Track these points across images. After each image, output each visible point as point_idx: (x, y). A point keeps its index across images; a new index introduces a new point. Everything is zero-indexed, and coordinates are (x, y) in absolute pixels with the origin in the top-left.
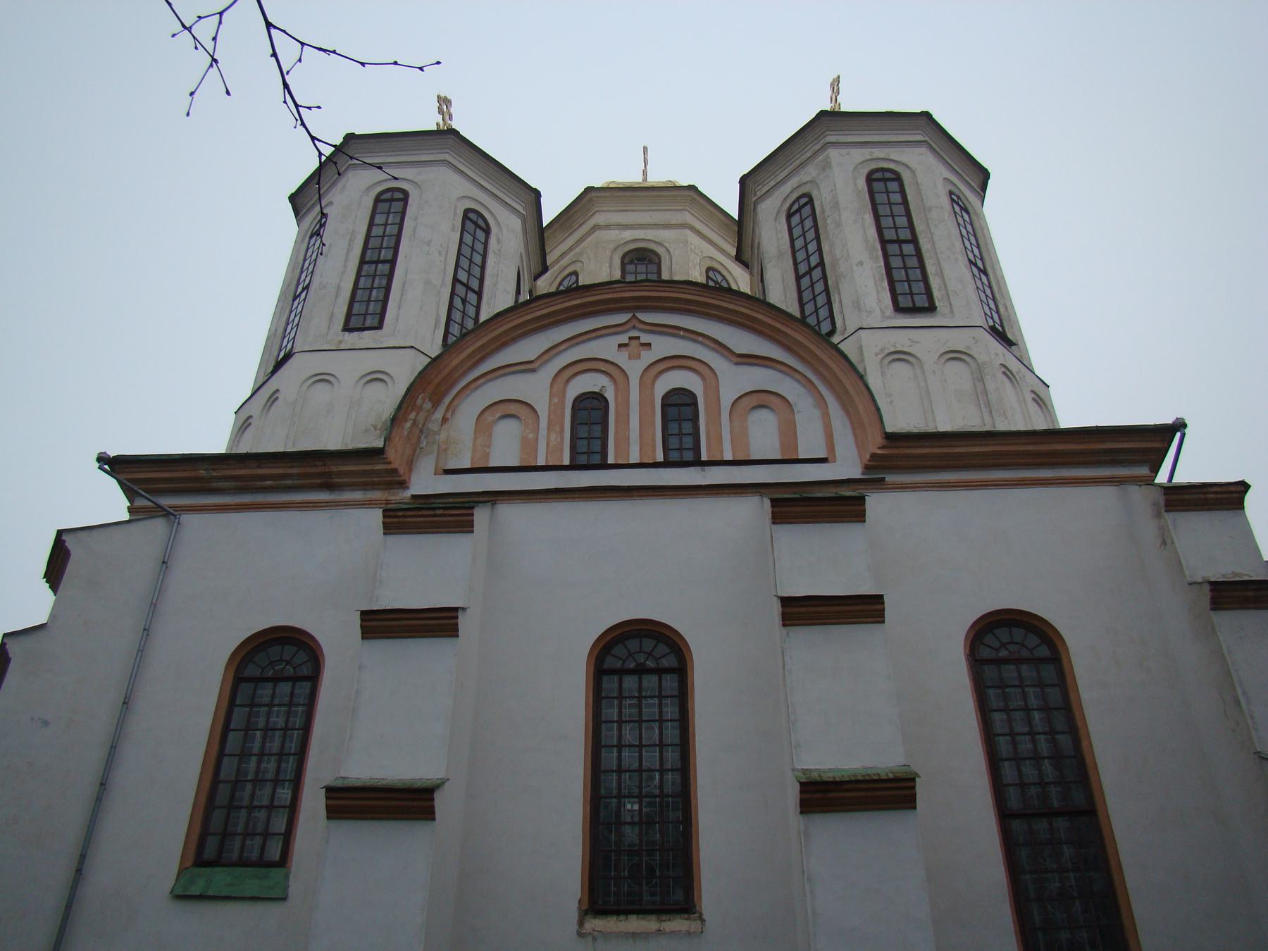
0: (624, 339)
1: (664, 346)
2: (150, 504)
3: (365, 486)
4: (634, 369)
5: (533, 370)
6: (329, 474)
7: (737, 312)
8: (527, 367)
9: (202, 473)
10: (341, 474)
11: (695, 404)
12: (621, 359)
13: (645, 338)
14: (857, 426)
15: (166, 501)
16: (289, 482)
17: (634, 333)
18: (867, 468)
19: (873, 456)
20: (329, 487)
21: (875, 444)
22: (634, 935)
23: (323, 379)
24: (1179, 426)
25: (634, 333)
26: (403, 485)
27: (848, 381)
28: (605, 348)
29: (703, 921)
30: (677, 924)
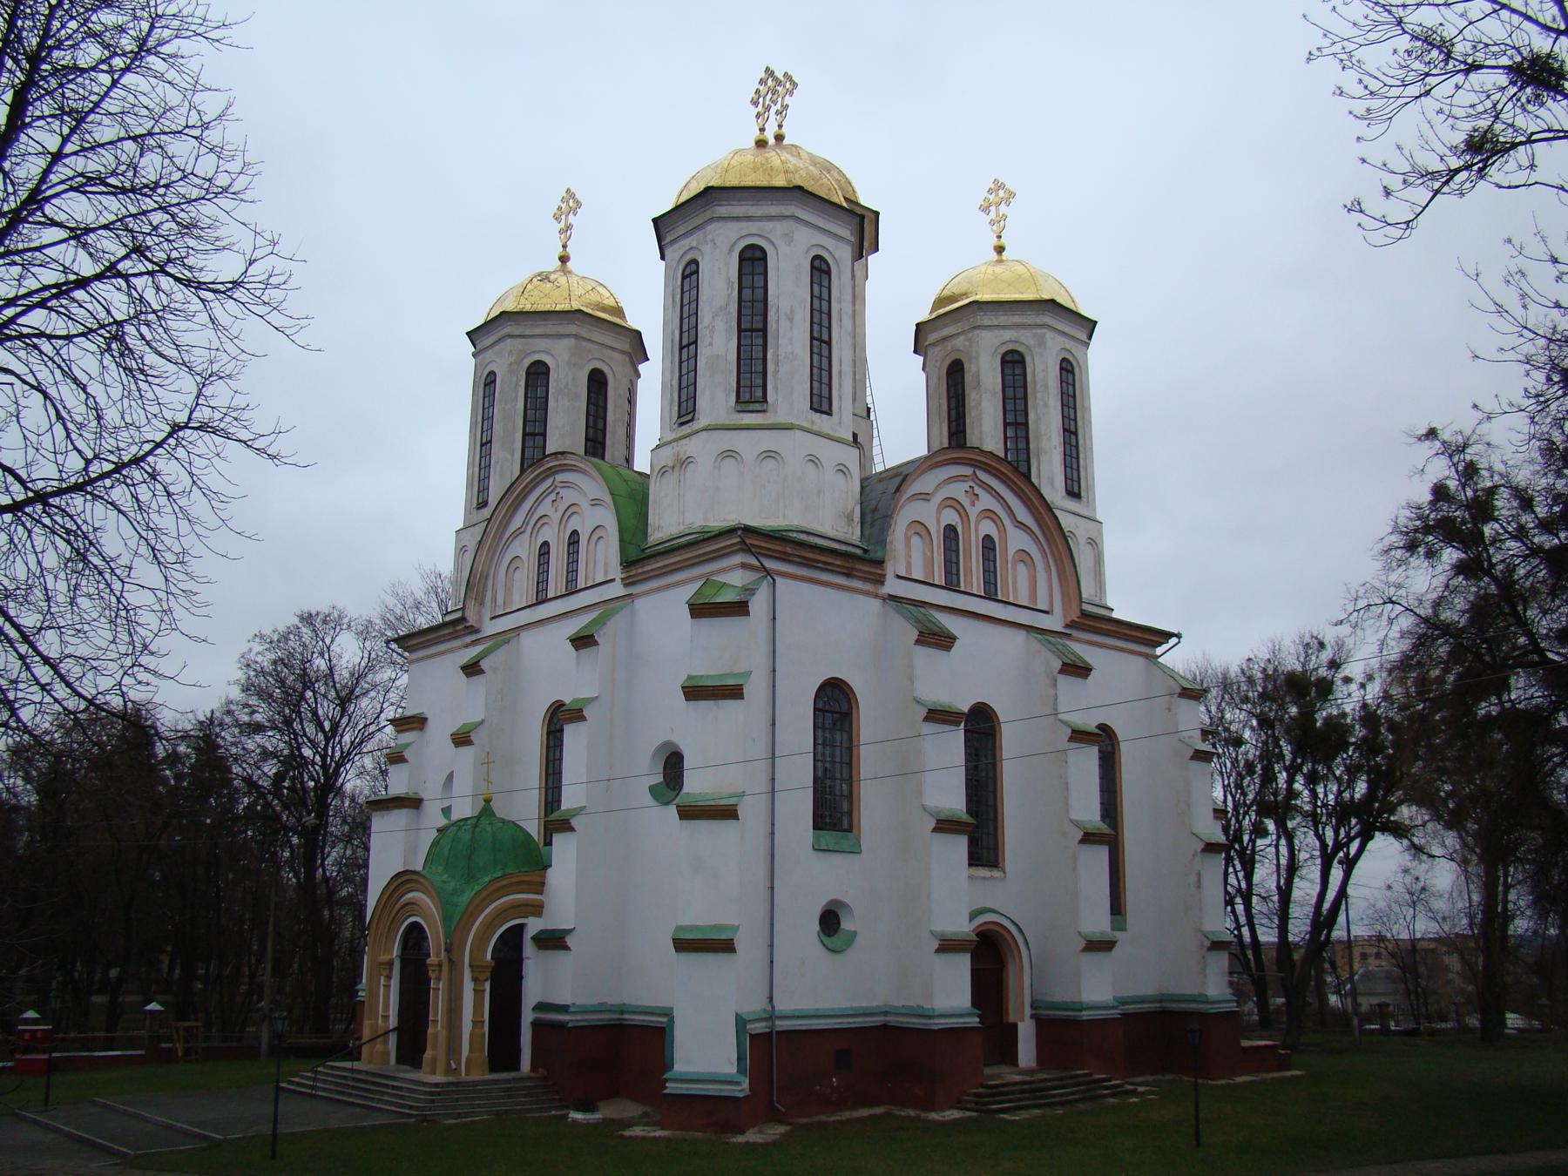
0: (966, 486)
1: (986, 501)
2: (758, 564)
3: (865, 580)
4: (973, 513)
5: (928, 500)
6: (852, 569)
7: (1023, 491)
8: (925, 497)
9: (789, 550)
10: (860, 571)
11: (994, 550)
12: (966, 503)
13: (977, 490)
14: (1065, 596)
15: (769, 564)
16: (830, 567)
17: (972, 484)
18: (1067, 626)
19: (1073, 621)
20: (848, 575)
21: (1074, 615)
22: (984, 878)
23: (813, 460)
24: (1178, 636)
25: (972, 484)
26: (882, 583)
27: (1067, 563)
28: (958, 491)
29: (1005, 873)
30: (996, 873)
